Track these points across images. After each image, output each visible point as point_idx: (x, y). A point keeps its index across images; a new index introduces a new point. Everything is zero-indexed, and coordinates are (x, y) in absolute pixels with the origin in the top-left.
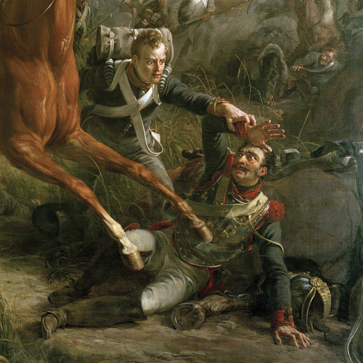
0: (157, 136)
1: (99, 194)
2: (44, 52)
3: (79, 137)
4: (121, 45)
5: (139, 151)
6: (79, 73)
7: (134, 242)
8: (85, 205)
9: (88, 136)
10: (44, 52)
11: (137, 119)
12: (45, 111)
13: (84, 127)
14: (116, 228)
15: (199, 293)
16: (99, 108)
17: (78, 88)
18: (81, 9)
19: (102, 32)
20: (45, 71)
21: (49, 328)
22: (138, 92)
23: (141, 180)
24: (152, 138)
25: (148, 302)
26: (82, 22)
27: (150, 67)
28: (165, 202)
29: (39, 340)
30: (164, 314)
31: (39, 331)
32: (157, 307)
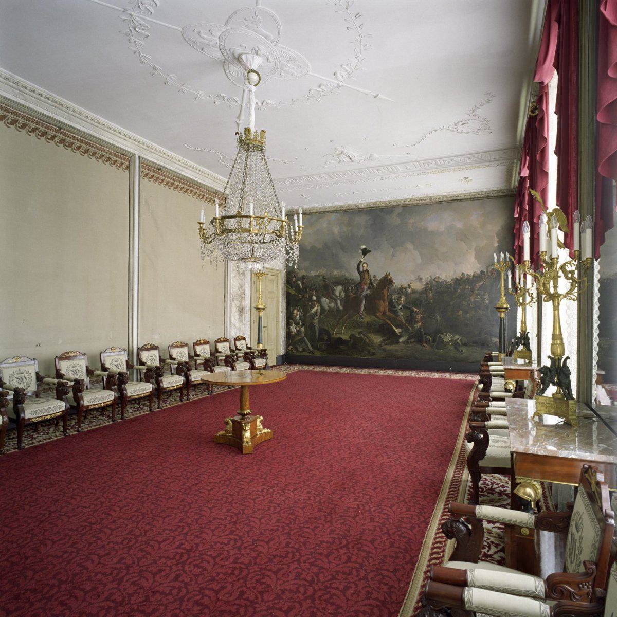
1: (391, 322)
3: (388, 313)
7: (398, 331)
8: (389, 324)
12: (382, 309)
14: (395, 328)
15: (408, 339)
20: (382, 302)
22: (399, 305)
30: (403, 342)
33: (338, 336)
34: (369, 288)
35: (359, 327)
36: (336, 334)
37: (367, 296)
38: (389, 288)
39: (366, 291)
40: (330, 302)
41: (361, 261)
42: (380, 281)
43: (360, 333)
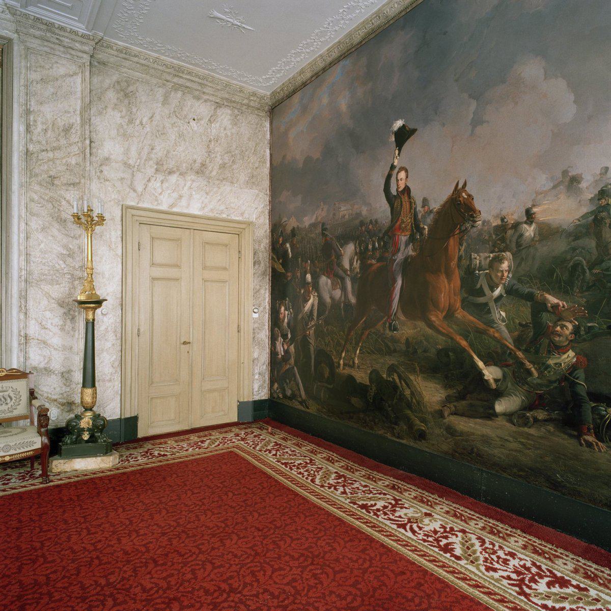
0: (503, 314)
1: (471, 345)
2: (443, 270)
3: (460, 314)
4: (483, 263)
5: (493, 322)
6: (460, 279)
7: (490, 373)
9: (465, 313)
10: (443, 270)
11: (492, 304)
13: (463, 308)
14: (481, 364)
16: (471, 298)
17: (460, 288)
18: (462, 245)
19: (473, 257)
20: (443, 279)
21: (446, 414)
22: (492, 289)
23: (494, 338)
24: (501, 314)
25: (499, 407)
26: (462, 252)
27: (500, 274)
28: (509, 351)
29: (441, 419)
31: (440, 414)
32: (504, 412)
33: (347, 371)
34: (412, 239)
35: (390, 352)
36: (345, 365)
37: (407, 264)
38: (464, 232)
39: (405, 251)
40: (334, 287)
41: (393, 167)
42: (439, 213)
43: (392, 369)
